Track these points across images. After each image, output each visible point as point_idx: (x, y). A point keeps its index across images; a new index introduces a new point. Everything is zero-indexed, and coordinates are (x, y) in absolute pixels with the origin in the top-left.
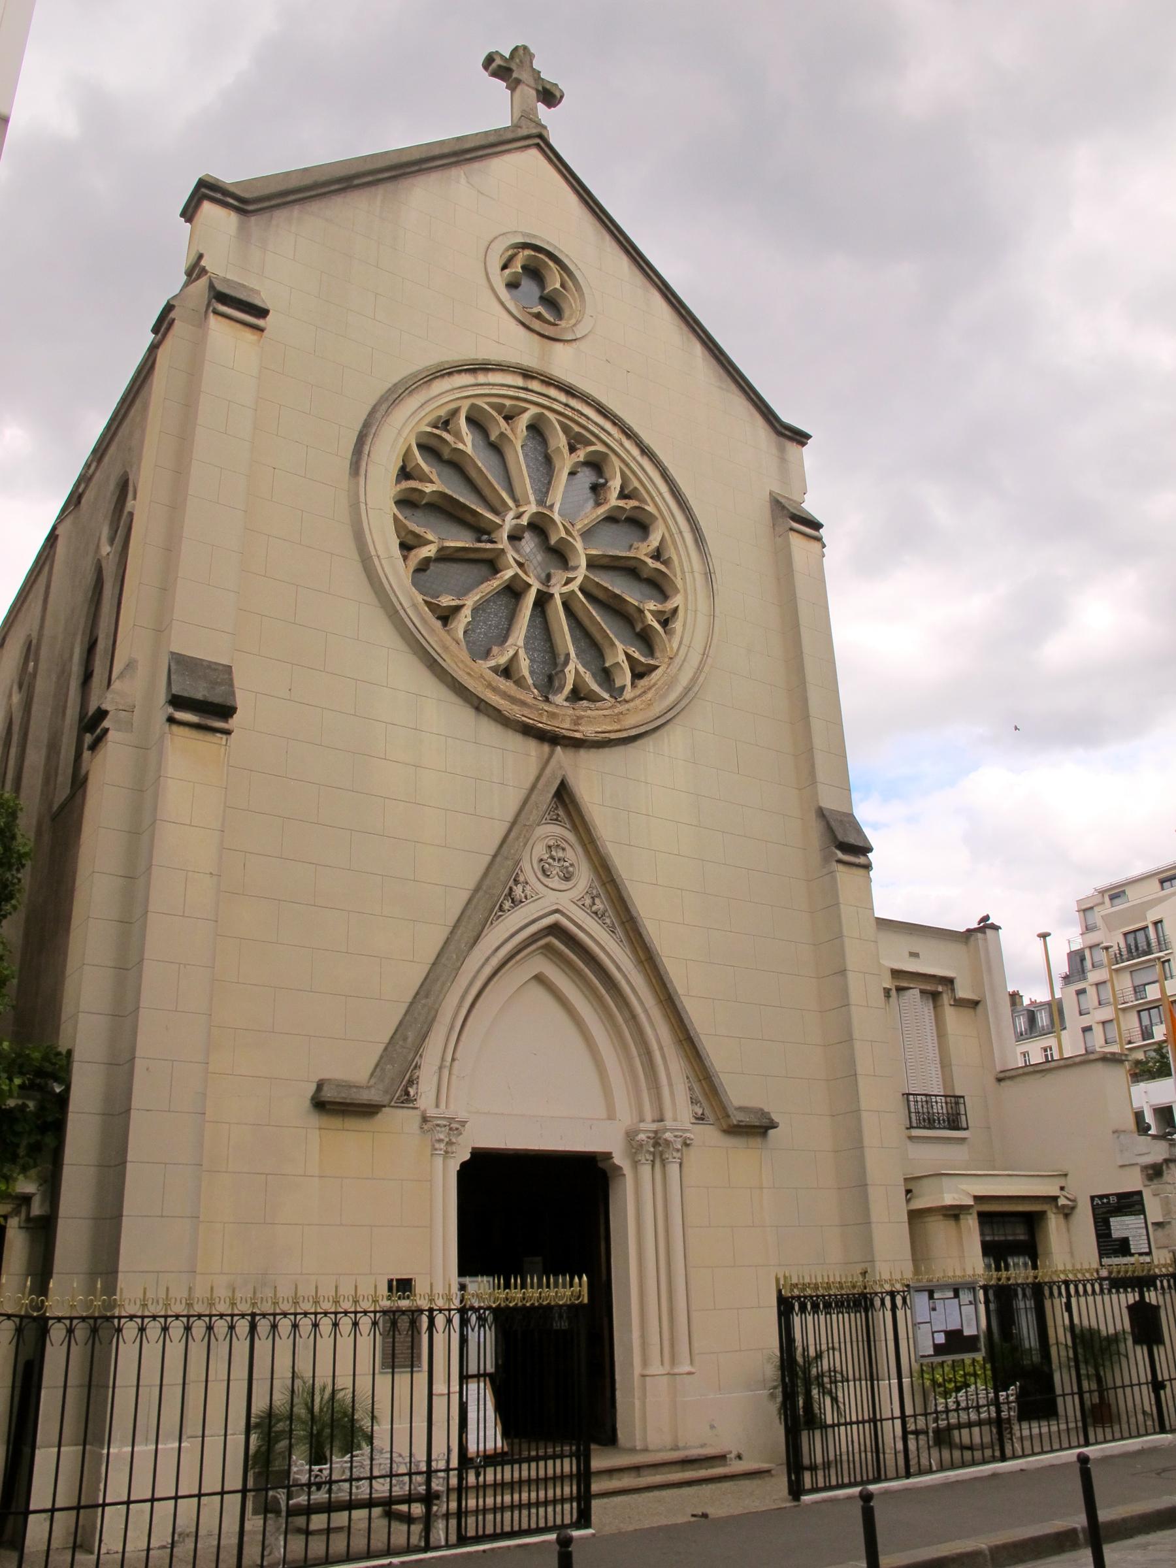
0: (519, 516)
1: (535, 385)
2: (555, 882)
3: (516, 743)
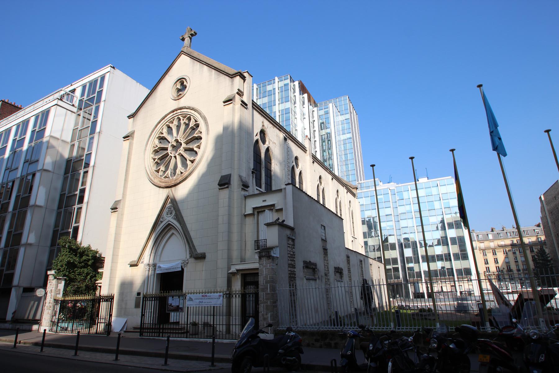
2: (169, 215)
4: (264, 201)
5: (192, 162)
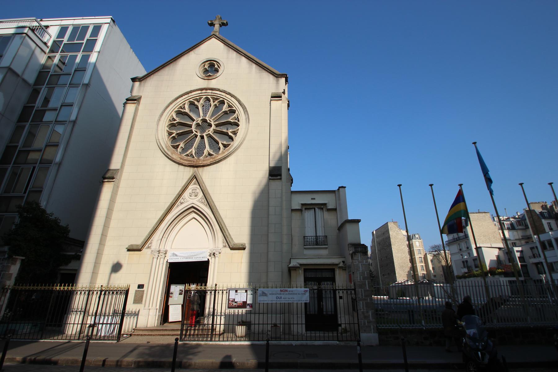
1: (204, 91)
2: (193, 197)
3: (188, 169)
5: (225, 146)
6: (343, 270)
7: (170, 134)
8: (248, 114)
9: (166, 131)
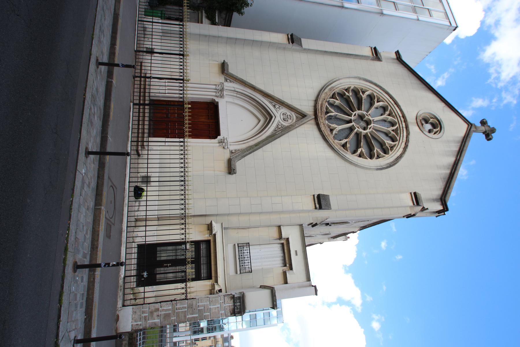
0: (367, 115)
4: (296, 251)
5: (344, 146)
6: (211, 290)
7: (347, 90)
8: (387, 168)
9: (349, 86)
